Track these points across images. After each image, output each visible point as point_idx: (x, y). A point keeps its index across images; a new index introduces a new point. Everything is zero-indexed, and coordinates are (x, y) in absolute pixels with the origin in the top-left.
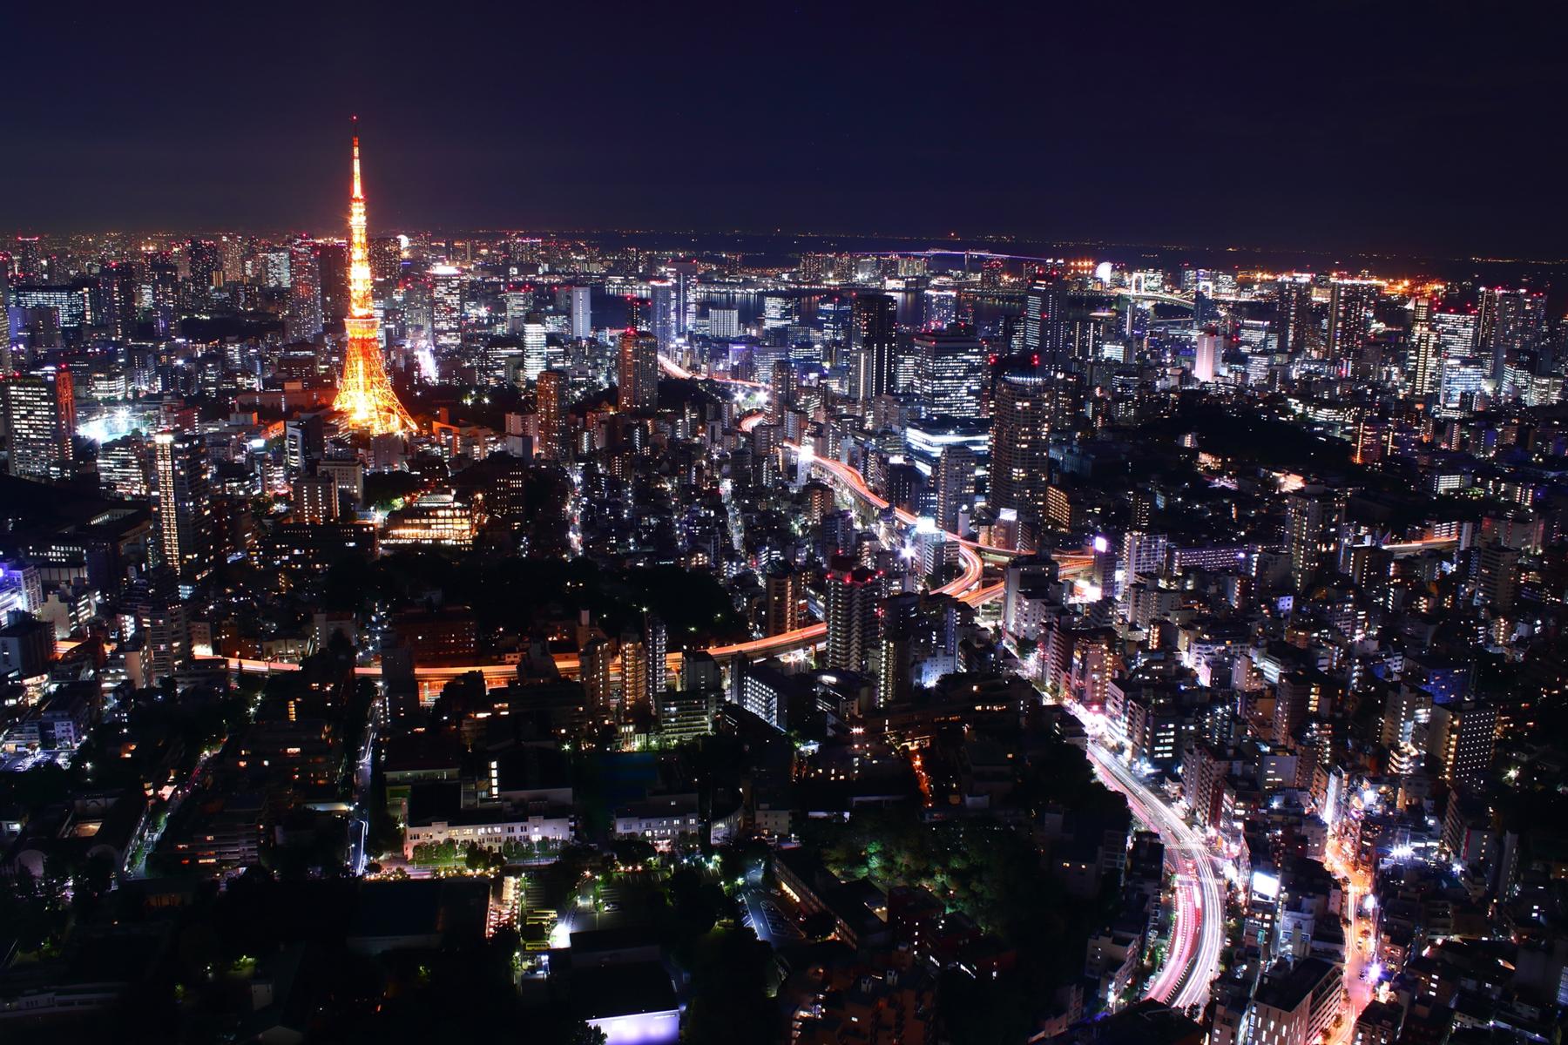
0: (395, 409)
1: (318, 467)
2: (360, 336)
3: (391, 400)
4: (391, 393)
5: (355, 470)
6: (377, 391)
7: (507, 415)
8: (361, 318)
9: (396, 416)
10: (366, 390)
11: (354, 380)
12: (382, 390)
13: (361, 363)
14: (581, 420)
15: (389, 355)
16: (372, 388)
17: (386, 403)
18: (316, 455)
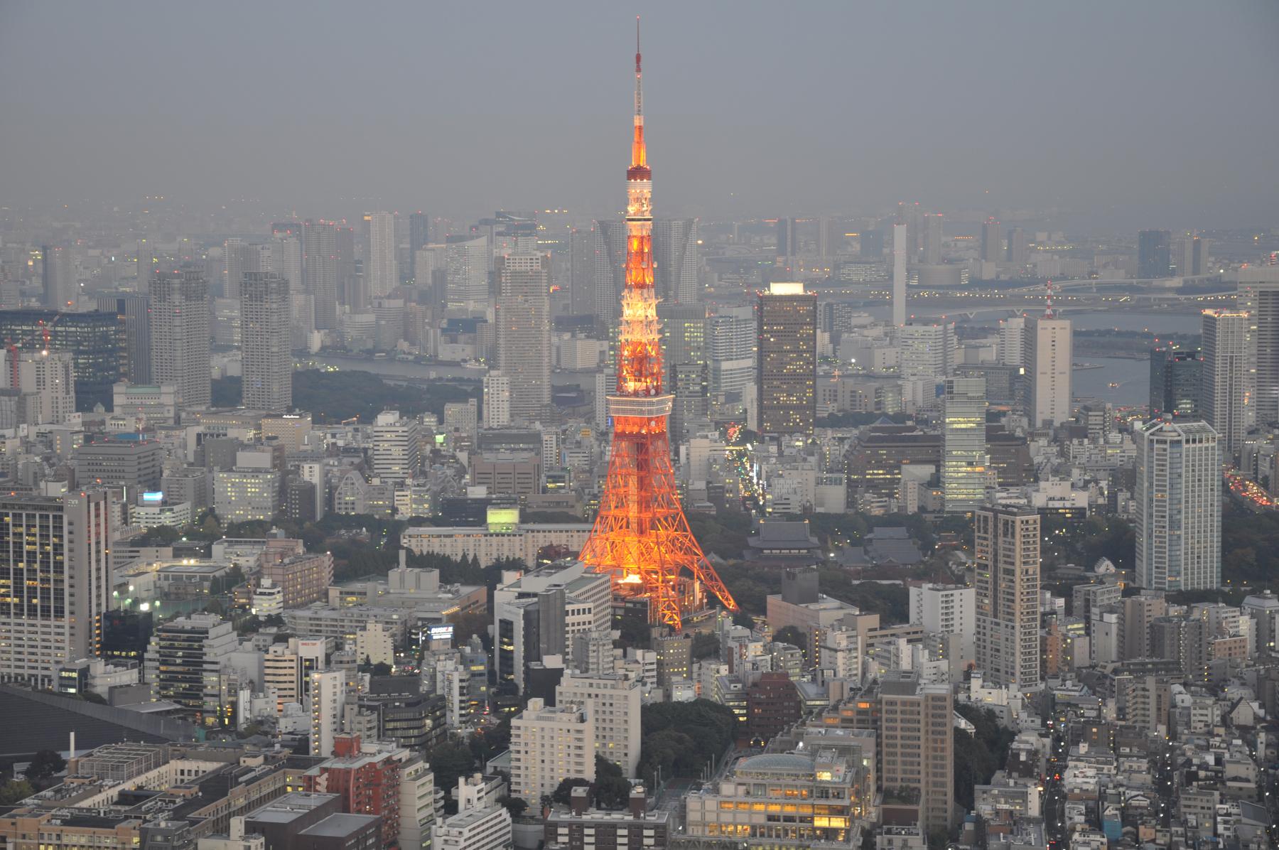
0: (695, 568)
1: (558, 688)
2: (636, 429)
3: (688, 551)
4: (688, 539)
5: (626, 697)
6: (662, 531)
7: (913, 591)
8: (636, 393)
9: (697, 585)
10: (641, 532)
11: (620, 513)
12: (673, 533)
13: (633, 482)
14: (1061, 602)
15: (677, 453)
16: (654, 527)
17: (680, 557)
18: (552, 661)
